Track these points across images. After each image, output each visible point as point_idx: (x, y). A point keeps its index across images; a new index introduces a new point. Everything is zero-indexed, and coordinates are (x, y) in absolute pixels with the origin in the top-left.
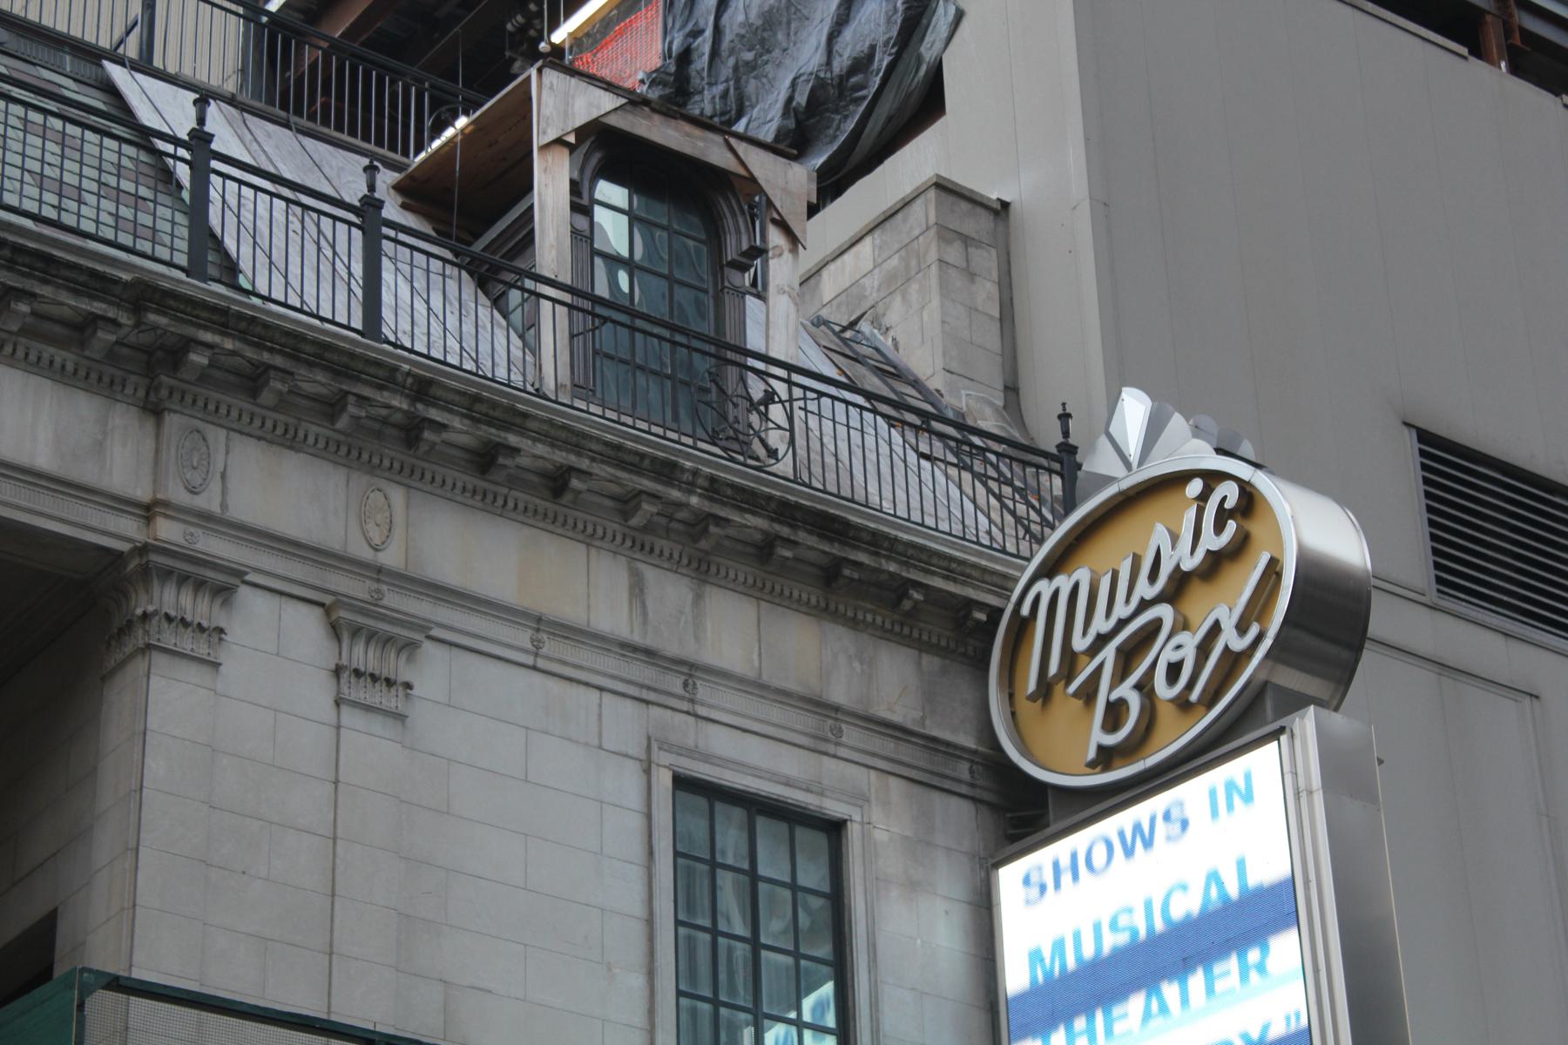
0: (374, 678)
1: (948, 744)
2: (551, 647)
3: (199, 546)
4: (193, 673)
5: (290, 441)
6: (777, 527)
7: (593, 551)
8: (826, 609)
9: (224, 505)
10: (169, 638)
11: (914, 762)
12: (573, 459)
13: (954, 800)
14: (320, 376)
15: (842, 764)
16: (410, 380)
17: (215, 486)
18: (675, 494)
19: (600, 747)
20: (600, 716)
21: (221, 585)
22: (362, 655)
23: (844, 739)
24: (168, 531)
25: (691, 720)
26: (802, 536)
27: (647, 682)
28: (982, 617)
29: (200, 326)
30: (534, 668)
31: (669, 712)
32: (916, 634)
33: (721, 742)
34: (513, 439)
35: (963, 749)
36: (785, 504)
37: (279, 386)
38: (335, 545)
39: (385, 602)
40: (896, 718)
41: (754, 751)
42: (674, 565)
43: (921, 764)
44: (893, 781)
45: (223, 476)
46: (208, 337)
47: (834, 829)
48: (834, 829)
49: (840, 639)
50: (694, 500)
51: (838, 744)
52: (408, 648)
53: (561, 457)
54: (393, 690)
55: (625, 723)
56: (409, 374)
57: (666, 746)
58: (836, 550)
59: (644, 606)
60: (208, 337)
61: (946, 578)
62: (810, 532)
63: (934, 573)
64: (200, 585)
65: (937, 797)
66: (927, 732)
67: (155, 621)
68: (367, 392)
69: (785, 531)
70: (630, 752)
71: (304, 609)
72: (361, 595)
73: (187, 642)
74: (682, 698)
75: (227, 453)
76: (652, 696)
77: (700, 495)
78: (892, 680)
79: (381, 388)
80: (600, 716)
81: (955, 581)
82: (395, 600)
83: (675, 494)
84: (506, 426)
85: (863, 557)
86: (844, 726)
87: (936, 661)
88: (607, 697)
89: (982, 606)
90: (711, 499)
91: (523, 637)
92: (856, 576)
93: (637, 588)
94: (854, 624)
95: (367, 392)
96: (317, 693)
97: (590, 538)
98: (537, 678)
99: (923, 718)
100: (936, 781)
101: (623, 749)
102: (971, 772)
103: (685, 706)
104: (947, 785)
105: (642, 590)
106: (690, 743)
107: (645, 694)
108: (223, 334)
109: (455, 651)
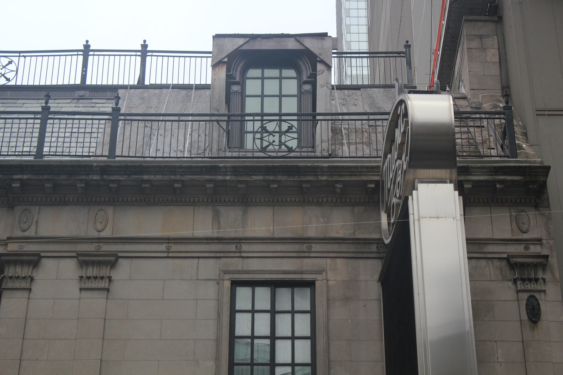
0: (95, 278)
1: (365, 239)
2: (174, 248)
3: (24, 249)
4: (19, 294)
5: (64, 203)
6: (267, 177)
7: (196, 208)
8: (304, 201)
9: (36, 232)
10: (10, 285)
11: (348, 250)
12: (173, 177)
13: (370, 261)
14: (63, 177)
15: (313, 259)
16: (98, 169)
17: (33, 227)
18: (220, 178)
19: (198, 280)
20: (198, 267)
21: (34, 261)
22: (91, 271)
23: (313, 250)
24: (13, 247)
25: (240, 260)
26: (279, 178)
27: (219, 250)
28: (373, 186)
29: (13, 174)
30: (168, 257)
31: (230, 259)
32: (348, 200)
33: (254, 264)
34: (146, 177)
35: (373, 239)
36: (267, 167)
37: (48, 185)
38: (82, 234)
39: (102, 249)
40: (340, 235)
41: (270, 265)
42: (232, 203)
43: (352, 250)
44: (339, 261)
45: (37, 222)
46: (18, 177)
47: (311, 284)
48: (311, 284)
49: (313, 212)
50: (228, 178)
51: (310, 252)
52: (113, 265)
53: (166, 178)
54: (97, 280)
55: (209, 268)
56: (97, 166)
57: (225, 272)
58: (296, 178)
59: (219, 221)
60: (18, 177)
61: (351, 175)
62: (283, 175)
63: (344, 175)
64: (22, 263)
65: (361, 262)
66: (356, 237)
67: (5, 280)
68: (83, 177)
69: (271, 178)
70: (211, 278)
71: (68, 261)
72: (91, 249)
73: (17, 284)
74: (236, 252)
75: (39, 214)
76: (222, 255)
77: (231, 175)
78: (339, 223)
79: (88, 174)
80: (198, 267)
81: (355, 175)
82: (106, 248)
83: (220, 178)
84: (142, 173)
85: (309, 178)
86: (312, 245)
87: (362, 208)
88: (201, 260)
89: (371, 182)
90: (236, 175)
91: (163, 247)
92: (309, 186)
93: (216, 217)
94: (319, 204)
95: (83, 177)
96: (73, 288)
97: (194, 204)
98: (170, 261)
99: (354, 232)
100: (360, 255)
101: (208, 278)
102: (377, 247)
103: (237, 255)
104: (365, 255)
105: (218, 217)
106: (240, 268)
107: (218, 255)
108: (23, 174)
109: (133, 260)
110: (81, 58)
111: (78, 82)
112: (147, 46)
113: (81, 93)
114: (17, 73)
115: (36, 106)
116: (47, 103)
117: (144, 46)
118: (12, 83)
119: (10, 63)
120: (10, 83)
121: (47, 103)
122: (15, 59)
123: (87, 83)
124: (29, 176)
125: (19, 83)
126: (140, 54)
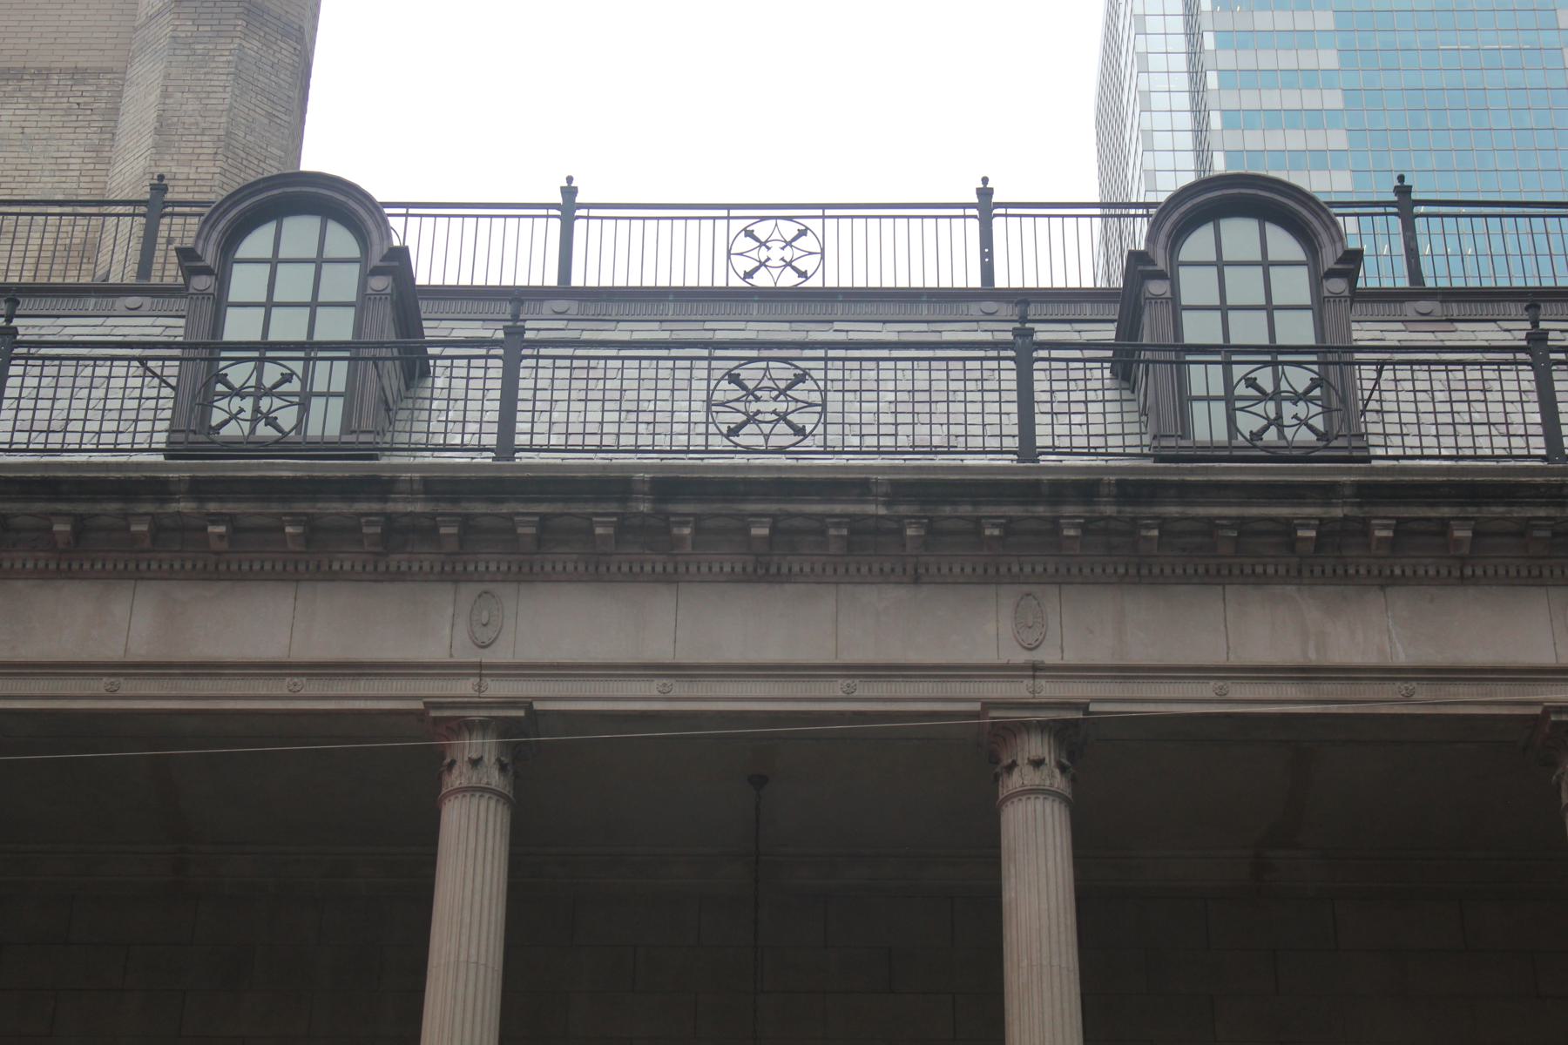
110: (556, 224)
111: (552, 280)
112: (1409, 190)
113: (560, 305)
114: (823, 258)
115: (1515, 332)
116: (1535, 324)
117: (985, 193)
118: (815, 282)
119: (802, 233)
120: (808, 284)
121: (1535, 324)
122: (815, 225)
123: (997, 285)
124: (1347, 510)
125: (831, 283)
126: (975, 212)
